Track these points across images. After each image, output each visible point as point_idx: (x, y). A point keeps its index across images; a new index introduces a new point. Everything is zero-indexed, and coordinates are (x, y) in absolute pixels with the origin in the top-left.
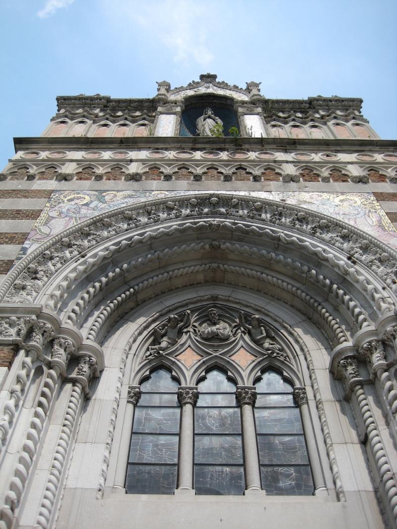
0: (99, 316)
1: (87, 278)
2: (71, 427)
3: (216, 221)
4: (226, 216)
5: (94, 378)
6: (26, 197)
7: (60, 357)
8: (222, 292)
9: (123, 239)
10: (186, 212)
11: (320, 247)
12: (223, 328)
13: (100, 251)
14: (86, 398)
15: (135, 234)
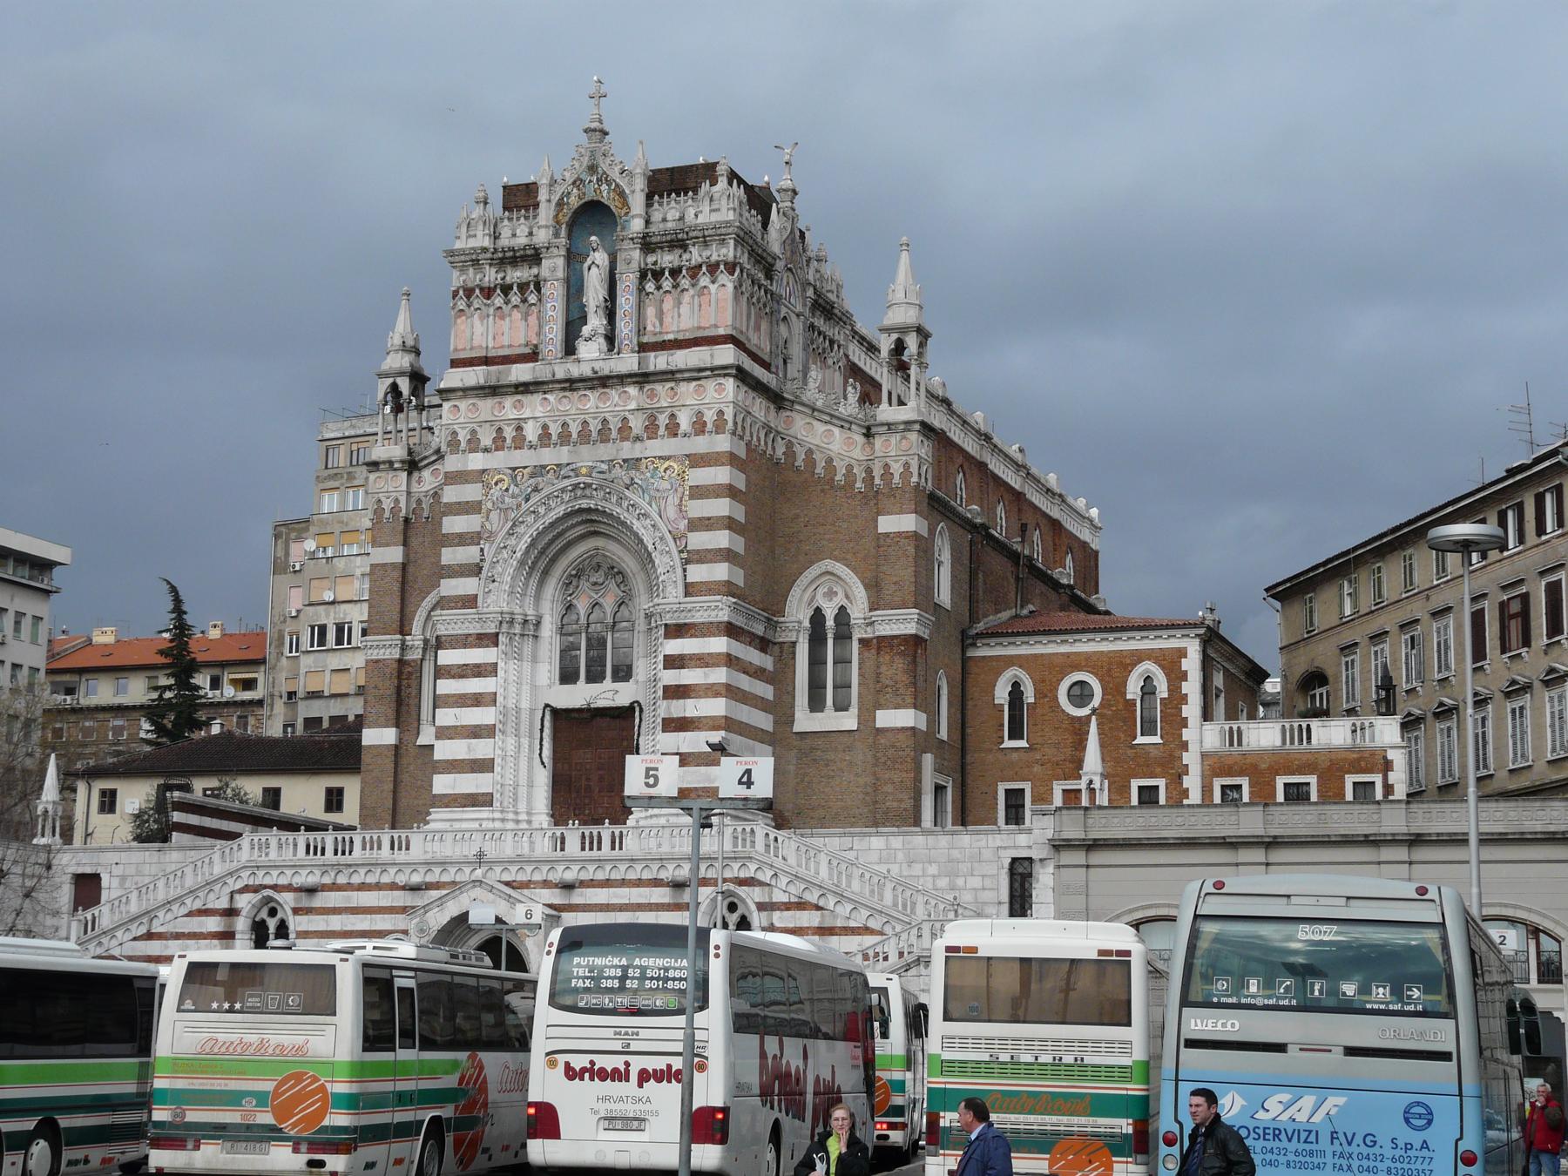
0: (533, 582)
1: (522, 563)
2: (535, 660)
3: (584, 503)
4: (591, 497)
5: (538, 624)
6: (467, 482)
7: (517, 629)
8: (599, 542)
9: (533, 531)
10: (566, 497)
11: (641, 532)
12: (598, 577)
13: (522, 546)
14: (536, 637)
15: (540, 525)
